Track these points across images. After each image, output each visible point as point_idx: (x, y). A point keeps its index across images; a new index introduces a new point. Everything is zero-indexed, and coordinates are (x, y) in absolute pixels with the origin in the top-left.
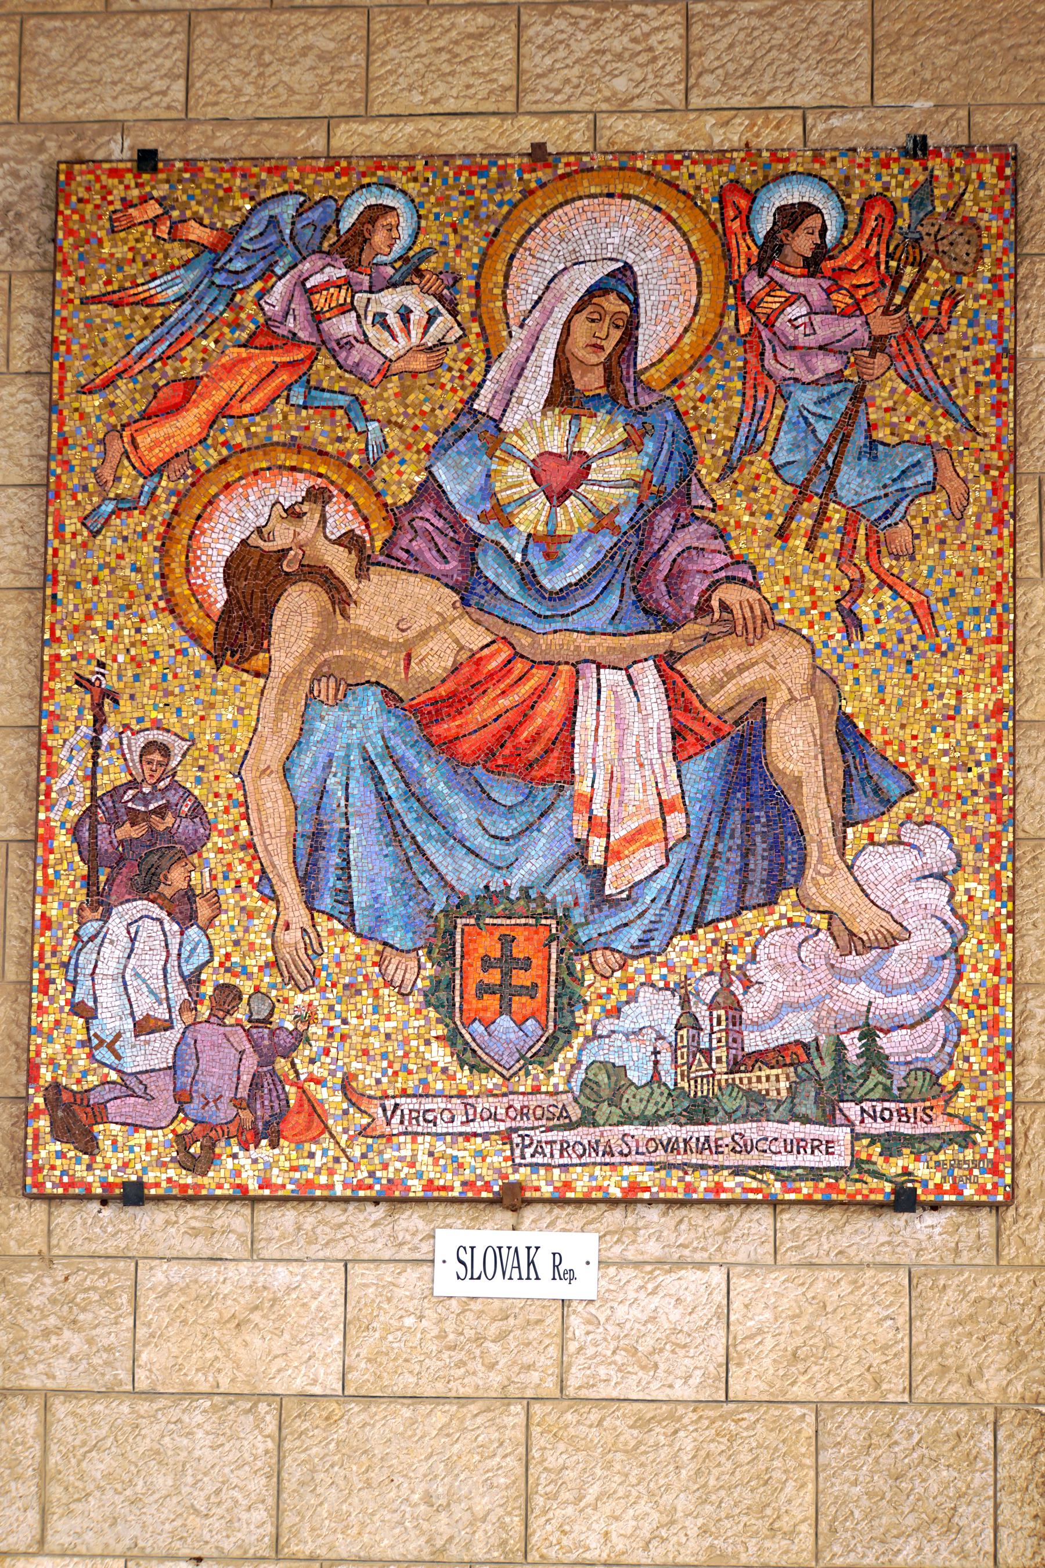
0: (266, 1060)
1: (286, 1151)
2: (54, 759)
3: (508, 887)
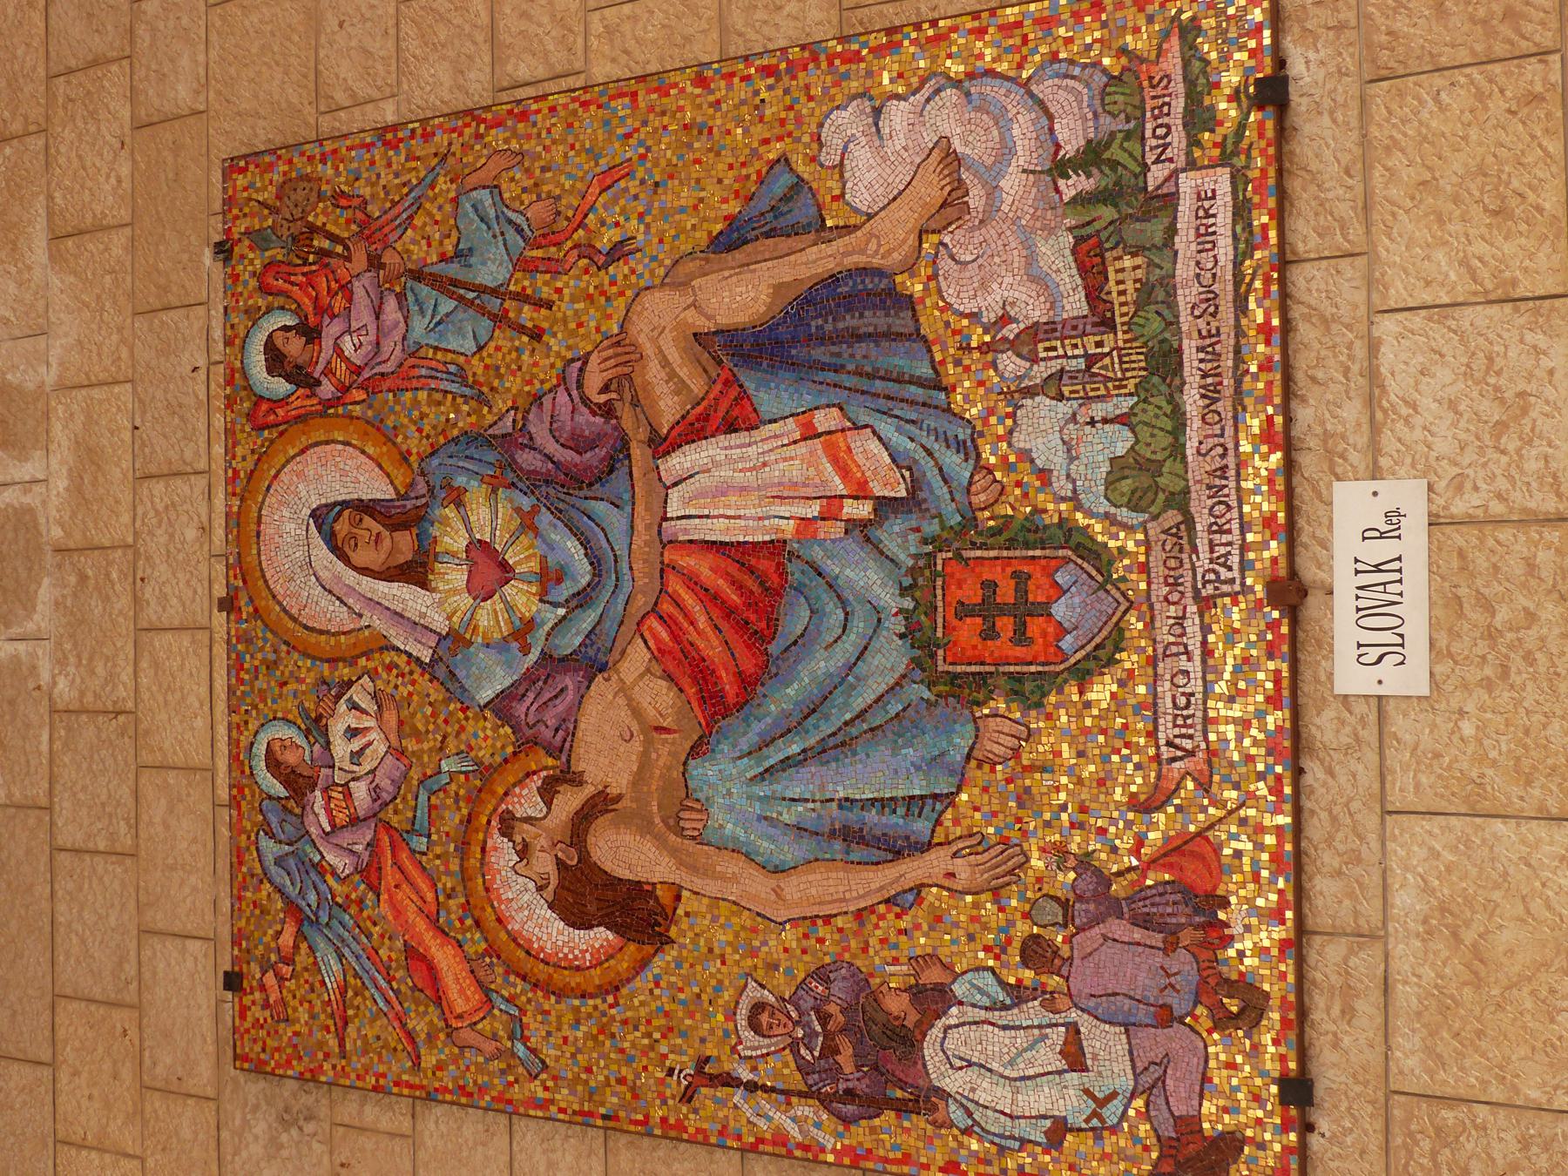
0: (1114, 908)
1: (1232, 887)
2: (768, 1136)
3: (900, 611)
